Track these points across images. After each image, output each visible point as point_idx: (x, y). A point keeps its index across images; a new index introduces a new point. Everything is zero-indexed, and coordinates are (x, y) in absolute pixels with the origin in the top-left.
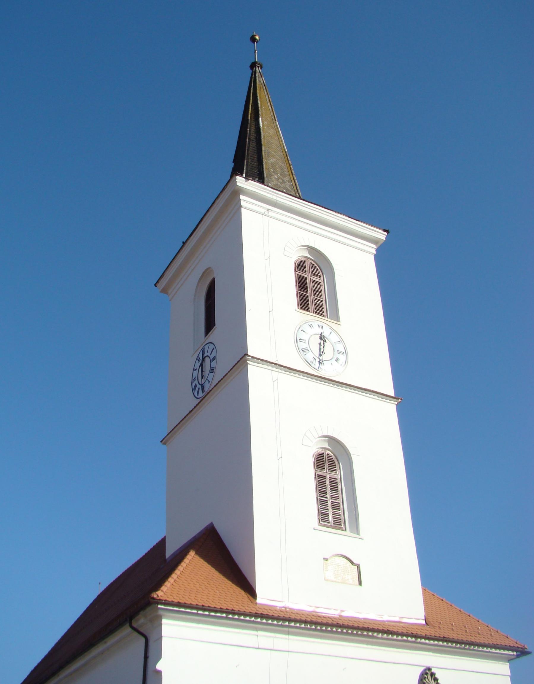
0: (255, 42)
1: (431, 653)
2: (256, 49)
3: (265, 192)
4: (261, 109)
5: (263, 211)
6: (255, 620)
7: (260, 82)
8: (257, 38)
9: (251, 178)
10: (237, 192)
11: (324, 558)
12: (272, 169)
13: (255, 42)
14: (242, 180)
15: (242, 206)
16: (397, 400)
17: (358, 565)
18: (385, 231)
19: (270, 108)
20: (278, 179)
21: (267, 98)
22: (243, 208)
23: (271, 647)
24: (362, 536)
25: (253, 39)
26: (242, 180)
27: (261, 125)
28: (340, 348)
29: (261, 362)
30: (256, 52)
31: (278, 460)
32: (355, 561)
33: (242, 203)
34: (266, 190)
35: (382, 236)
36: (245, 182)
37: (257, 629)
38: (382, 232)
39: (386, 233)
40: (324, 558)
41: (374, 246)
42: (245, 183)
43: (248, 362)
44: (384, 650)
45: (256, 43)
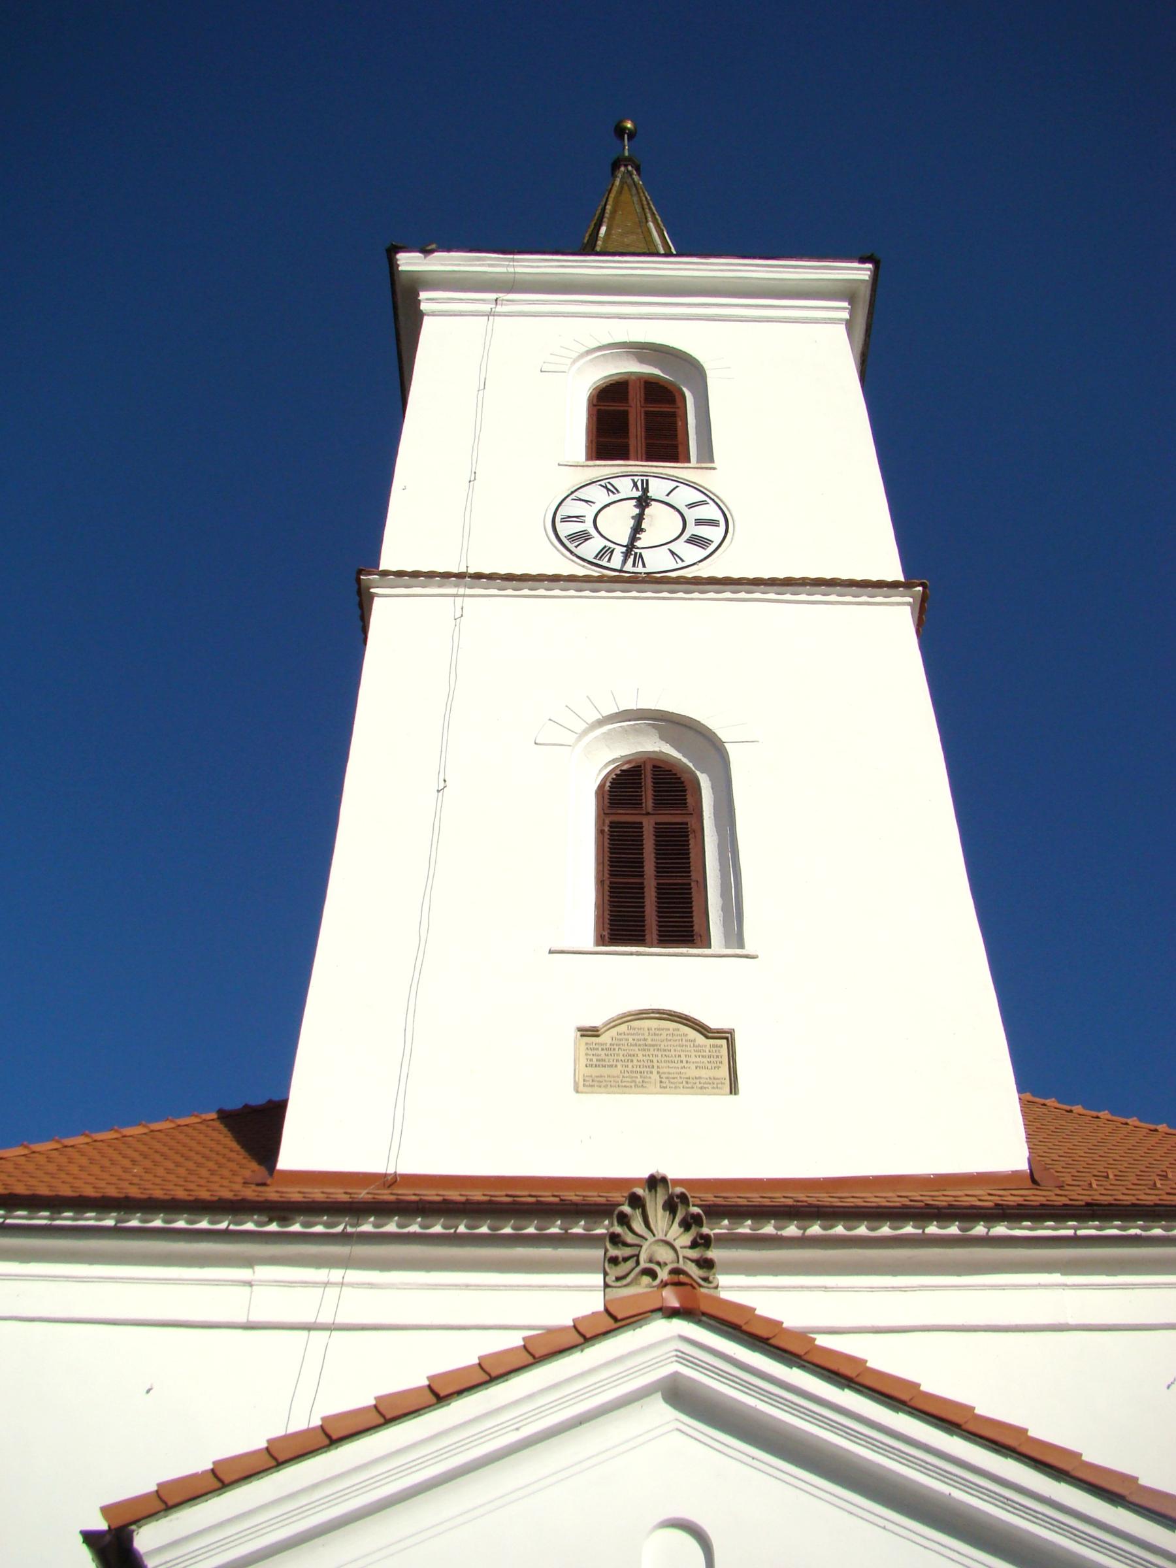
0: (626, 136)
1: (1056, 1278)
3: (483, 265)
5: (486, 308)
6: (232, 1227)
8: (629, 125)
9: (434, 246)
11: (580, 1029)
13: (626, 136)
14: (418, 258)
15: (424, 311)
16: (907, 592)
17: (729, 1035)
18: (863, 260)
22: (429, 315)
23: (309, 1318)
24: (749, 949)
25: (620, 131)
26: (418, 258)
28: (710, 512)
29: (414, 581)
30: (627, 147)
31: (438, 791)
32: (713, 1023)
33: (424, 307)
34: (484, 261)
35: (860, 273)
36: (425, 257)
37: (249, 1262)
39: (870, 266)
40: (580, 1029)
41: (845, 304)
42: (425, 262)
43: (372, 590)
44: (825, 1288)
45: (629, 140)
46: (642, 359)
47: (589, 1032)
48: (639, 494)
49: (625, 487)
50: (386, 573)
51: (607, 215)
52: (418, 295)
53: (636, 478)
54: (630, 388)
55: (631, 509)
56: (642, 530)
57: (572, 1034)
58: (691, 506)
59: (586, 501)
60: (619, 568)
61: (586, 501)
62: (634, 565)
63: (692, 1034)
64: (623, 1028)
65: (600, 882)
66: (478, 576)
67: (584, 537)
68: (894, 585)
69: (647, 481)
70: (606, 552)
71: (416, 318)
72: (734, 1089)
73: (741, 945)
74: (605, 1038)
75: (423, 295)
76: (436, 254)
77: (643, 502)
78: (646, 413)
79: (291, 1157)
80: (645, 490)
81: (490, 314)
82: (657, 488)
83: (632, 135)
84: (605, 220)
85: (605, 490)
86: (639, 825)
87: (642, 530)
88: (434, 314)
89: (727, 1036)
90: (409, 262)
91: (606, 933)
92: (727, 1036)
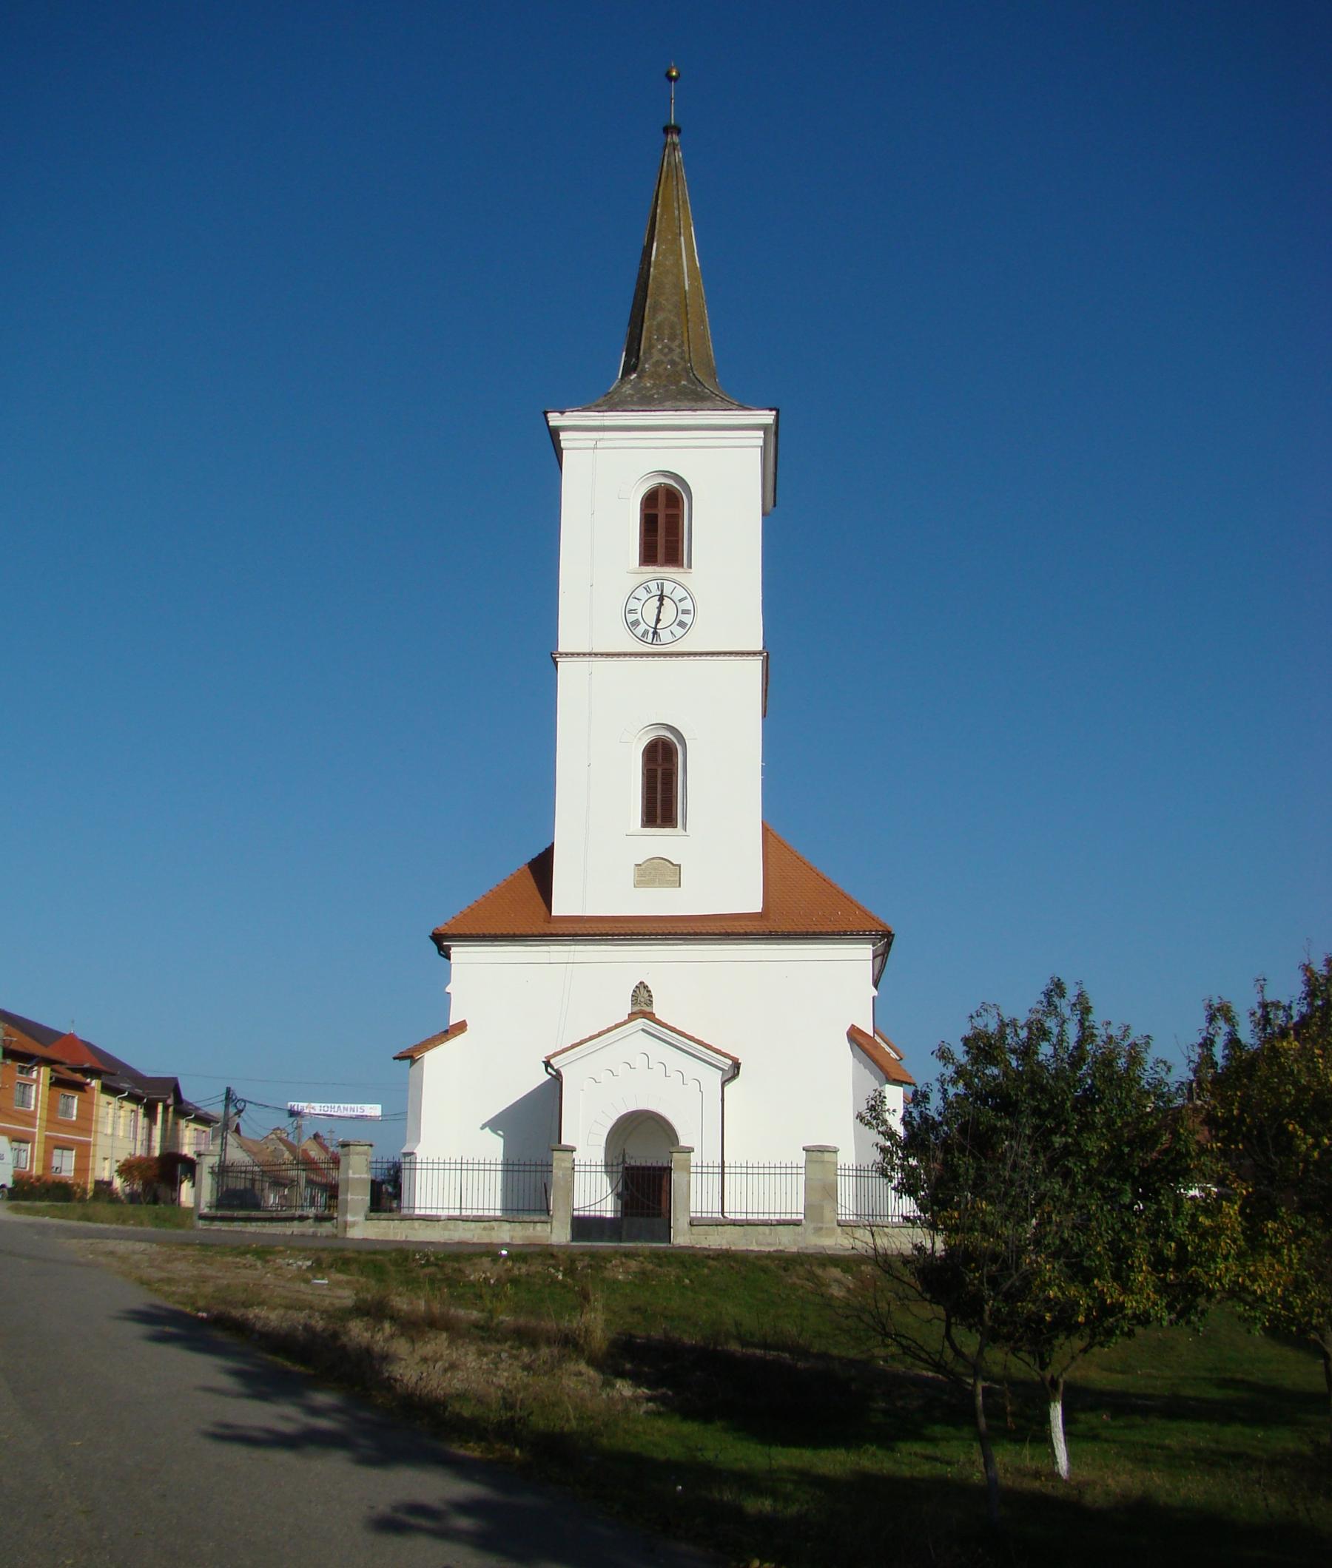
0: (673, 83)
2: (673, 96)
4: (661, 223)
5: (592, 444)
7: (669, 163)
10: (554, 433)
12: (655, 335)
13: (673, 83)
14: (558, 417)
18: (771, 410)
19: (677, 212)
20: (661, 351)
21: (675, 193)
25: (670, 78)
27: (653, 258)
28: (687, 605)
35: (767, 417)
38: (767, 412)
39: (774, 413)
43: (557, 660)
46: (665, 476)
47: (636, 865)
48: (659, 593)
49: (653, 586)
50: (561, 654)
51: (658, 216)
52: (559, 436)
53: (659, 581)
54: (660, 494)
55: (655, 602)
56: (660, 620)
57: (633, 866)
58: (680, 601)
59: (638, 599)
60: (650, 642)
61: (638, 599)
62: (657, 640)
63: (669, 865)
64: (647, 863)
65: (643, 797)
66: (596, 654)
67: (636, 623)
68: (754, 653)
69: (662, 584)
70: (646, 632)
71: (561, 450)
72: (680, 886)
73: (686, 831)
74: (643, 867)
75: (563, 435)
76: (567, 414)
77: (661, 598)
78: (667, 515)
79: (556, 911)
80: (662, 591)
81: (595, 448)
82: (668, 587)
83: (675, 79)
84: (655, 239)
85: (645, 591)
86: (656, 770)
87: (660, 620)
88: (568, 449)
89: (679, 866)
90: (555, 419)
91: (645, 819)
92: (679, 866)
